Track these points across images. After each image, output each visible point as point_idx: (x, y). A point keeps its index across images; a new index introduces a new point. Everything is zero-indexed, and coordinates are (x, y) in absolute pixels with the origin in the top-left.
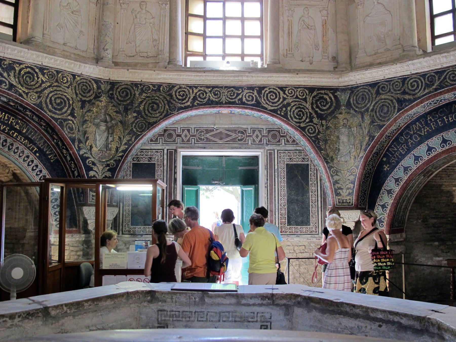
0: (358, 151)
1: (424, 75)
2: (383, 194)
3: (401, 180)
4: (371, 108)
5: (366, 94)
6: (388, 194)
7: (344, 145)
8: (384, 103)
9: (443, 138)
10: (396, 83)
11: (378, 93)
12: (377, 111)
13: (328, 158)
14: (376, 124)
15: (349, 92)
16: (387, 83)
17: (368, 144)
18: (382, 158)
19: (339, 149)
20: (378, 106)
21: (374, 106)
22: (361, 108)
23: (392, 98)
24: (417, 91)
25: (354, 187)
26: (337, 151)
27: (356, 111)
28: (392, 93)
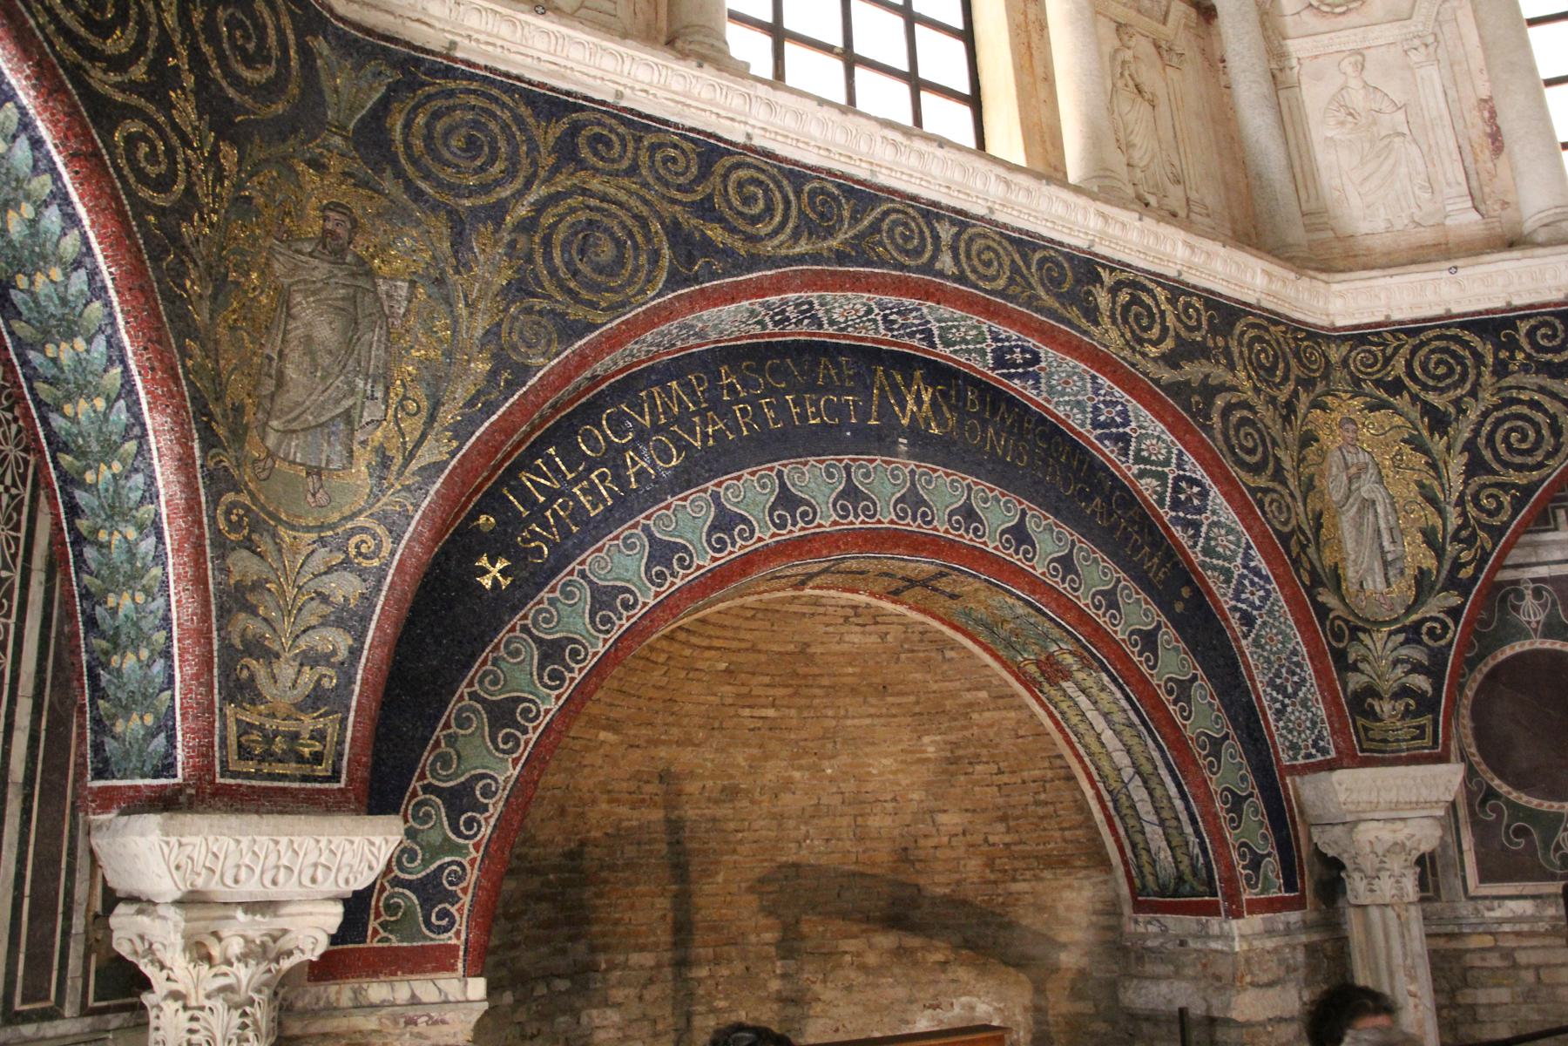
0: (412, 427)
1: (797, 174)
2: (463, 723)
3: (575, 653)
4: (523, 211)
5: (493, 126)
6: (495, 726)
7: (315, 364)
8: (597, 216)
9: (783, 485)
10: (672, 152)
11: (567, 152)
12: (559, 237)
13: (217, 410)
14: (546, 304)
15: (392, 76)
16: (622, 130)
17: (479, 404)
18: (474, 516)
19: (281, 374)
20: (561, 218)
21: (540, 207)
22: (455, 190)
23: (645, 211)
24: (762, 229)
25: (355, 653)
26: (269, 385)
27: (418, 195)
28: (645, 185)
